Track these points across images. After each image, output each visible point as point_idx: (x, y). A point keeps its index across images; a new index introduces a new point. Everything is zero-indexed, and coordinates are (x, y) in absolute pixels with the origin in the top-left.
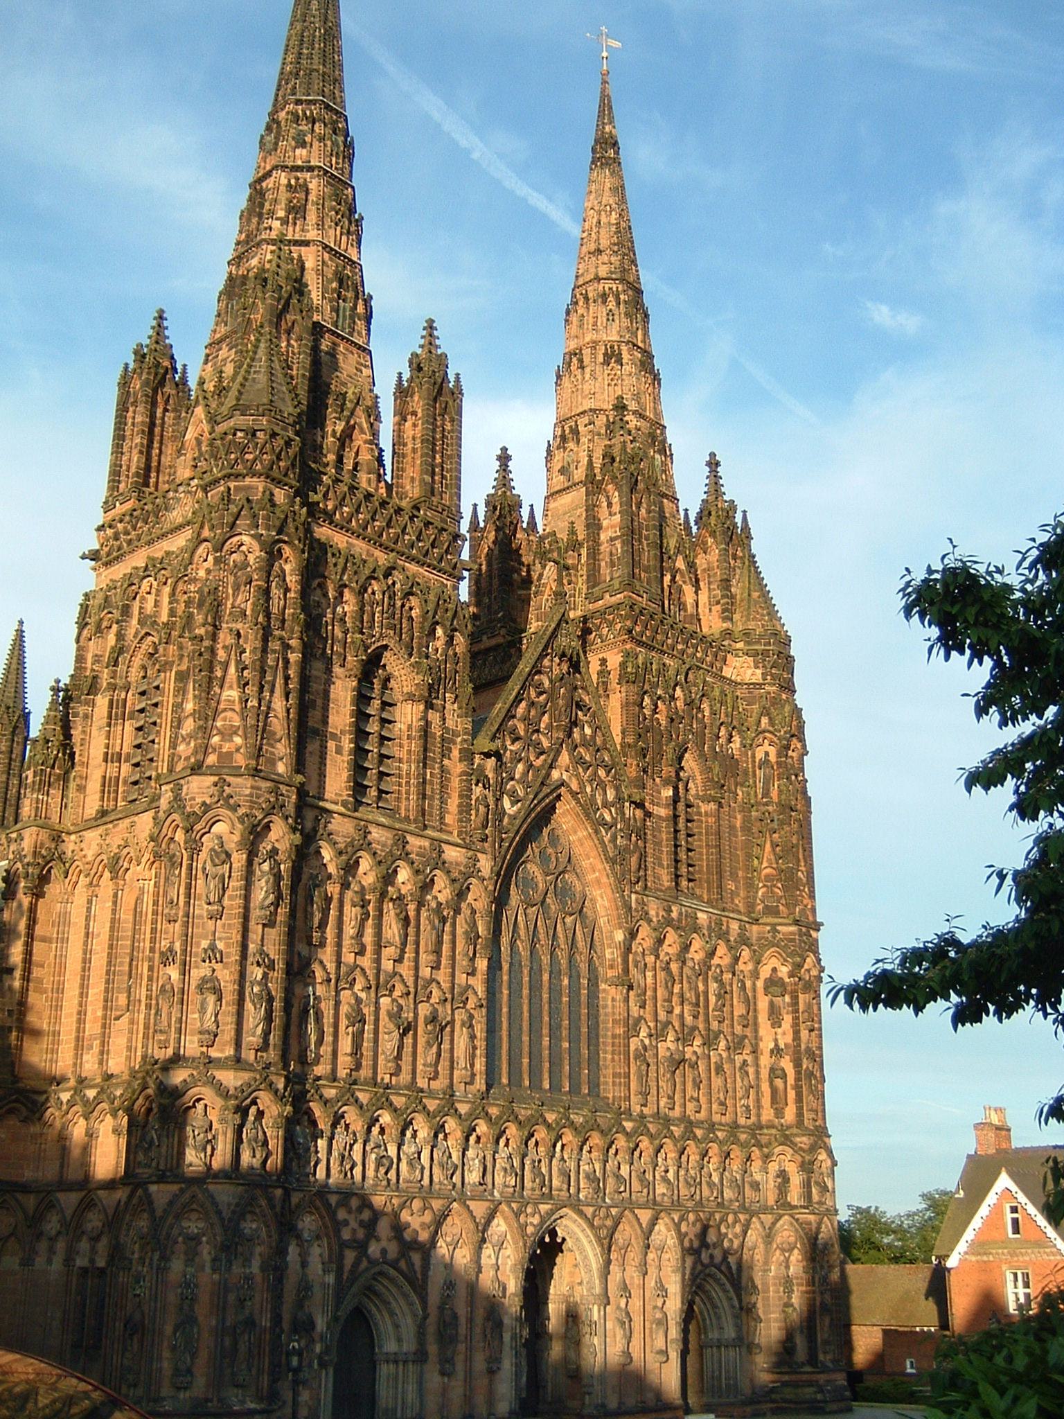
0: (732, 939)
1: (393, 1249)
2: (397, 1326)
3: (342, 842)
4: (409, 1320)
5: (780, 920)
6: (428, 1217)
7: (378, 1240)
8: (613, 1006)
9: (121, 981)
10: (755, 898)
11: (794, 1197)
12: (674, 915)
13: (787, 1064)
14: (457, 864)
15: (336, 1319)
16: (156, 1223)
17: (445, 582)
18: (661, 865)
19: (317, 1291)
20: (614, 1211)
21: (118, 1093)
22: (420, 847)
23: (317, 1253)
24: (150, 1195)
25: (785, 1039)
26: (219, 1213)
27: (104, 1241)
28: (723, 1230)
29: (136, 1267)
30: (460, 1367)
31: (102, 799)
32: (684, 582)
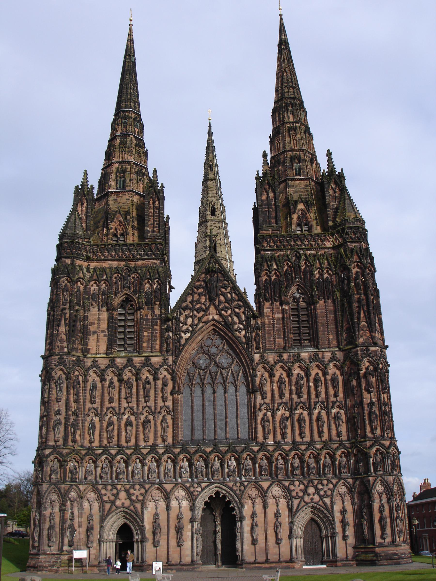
0: (326, 360)
1: (127, 503)
3: (103, 367)
6: (143, 491)
12: (285, 356)
13: (375, 409)
14: (158, 363)
17: (156, 262)
18: (279, 338)
22: (140, 361)
28: (320, 486)
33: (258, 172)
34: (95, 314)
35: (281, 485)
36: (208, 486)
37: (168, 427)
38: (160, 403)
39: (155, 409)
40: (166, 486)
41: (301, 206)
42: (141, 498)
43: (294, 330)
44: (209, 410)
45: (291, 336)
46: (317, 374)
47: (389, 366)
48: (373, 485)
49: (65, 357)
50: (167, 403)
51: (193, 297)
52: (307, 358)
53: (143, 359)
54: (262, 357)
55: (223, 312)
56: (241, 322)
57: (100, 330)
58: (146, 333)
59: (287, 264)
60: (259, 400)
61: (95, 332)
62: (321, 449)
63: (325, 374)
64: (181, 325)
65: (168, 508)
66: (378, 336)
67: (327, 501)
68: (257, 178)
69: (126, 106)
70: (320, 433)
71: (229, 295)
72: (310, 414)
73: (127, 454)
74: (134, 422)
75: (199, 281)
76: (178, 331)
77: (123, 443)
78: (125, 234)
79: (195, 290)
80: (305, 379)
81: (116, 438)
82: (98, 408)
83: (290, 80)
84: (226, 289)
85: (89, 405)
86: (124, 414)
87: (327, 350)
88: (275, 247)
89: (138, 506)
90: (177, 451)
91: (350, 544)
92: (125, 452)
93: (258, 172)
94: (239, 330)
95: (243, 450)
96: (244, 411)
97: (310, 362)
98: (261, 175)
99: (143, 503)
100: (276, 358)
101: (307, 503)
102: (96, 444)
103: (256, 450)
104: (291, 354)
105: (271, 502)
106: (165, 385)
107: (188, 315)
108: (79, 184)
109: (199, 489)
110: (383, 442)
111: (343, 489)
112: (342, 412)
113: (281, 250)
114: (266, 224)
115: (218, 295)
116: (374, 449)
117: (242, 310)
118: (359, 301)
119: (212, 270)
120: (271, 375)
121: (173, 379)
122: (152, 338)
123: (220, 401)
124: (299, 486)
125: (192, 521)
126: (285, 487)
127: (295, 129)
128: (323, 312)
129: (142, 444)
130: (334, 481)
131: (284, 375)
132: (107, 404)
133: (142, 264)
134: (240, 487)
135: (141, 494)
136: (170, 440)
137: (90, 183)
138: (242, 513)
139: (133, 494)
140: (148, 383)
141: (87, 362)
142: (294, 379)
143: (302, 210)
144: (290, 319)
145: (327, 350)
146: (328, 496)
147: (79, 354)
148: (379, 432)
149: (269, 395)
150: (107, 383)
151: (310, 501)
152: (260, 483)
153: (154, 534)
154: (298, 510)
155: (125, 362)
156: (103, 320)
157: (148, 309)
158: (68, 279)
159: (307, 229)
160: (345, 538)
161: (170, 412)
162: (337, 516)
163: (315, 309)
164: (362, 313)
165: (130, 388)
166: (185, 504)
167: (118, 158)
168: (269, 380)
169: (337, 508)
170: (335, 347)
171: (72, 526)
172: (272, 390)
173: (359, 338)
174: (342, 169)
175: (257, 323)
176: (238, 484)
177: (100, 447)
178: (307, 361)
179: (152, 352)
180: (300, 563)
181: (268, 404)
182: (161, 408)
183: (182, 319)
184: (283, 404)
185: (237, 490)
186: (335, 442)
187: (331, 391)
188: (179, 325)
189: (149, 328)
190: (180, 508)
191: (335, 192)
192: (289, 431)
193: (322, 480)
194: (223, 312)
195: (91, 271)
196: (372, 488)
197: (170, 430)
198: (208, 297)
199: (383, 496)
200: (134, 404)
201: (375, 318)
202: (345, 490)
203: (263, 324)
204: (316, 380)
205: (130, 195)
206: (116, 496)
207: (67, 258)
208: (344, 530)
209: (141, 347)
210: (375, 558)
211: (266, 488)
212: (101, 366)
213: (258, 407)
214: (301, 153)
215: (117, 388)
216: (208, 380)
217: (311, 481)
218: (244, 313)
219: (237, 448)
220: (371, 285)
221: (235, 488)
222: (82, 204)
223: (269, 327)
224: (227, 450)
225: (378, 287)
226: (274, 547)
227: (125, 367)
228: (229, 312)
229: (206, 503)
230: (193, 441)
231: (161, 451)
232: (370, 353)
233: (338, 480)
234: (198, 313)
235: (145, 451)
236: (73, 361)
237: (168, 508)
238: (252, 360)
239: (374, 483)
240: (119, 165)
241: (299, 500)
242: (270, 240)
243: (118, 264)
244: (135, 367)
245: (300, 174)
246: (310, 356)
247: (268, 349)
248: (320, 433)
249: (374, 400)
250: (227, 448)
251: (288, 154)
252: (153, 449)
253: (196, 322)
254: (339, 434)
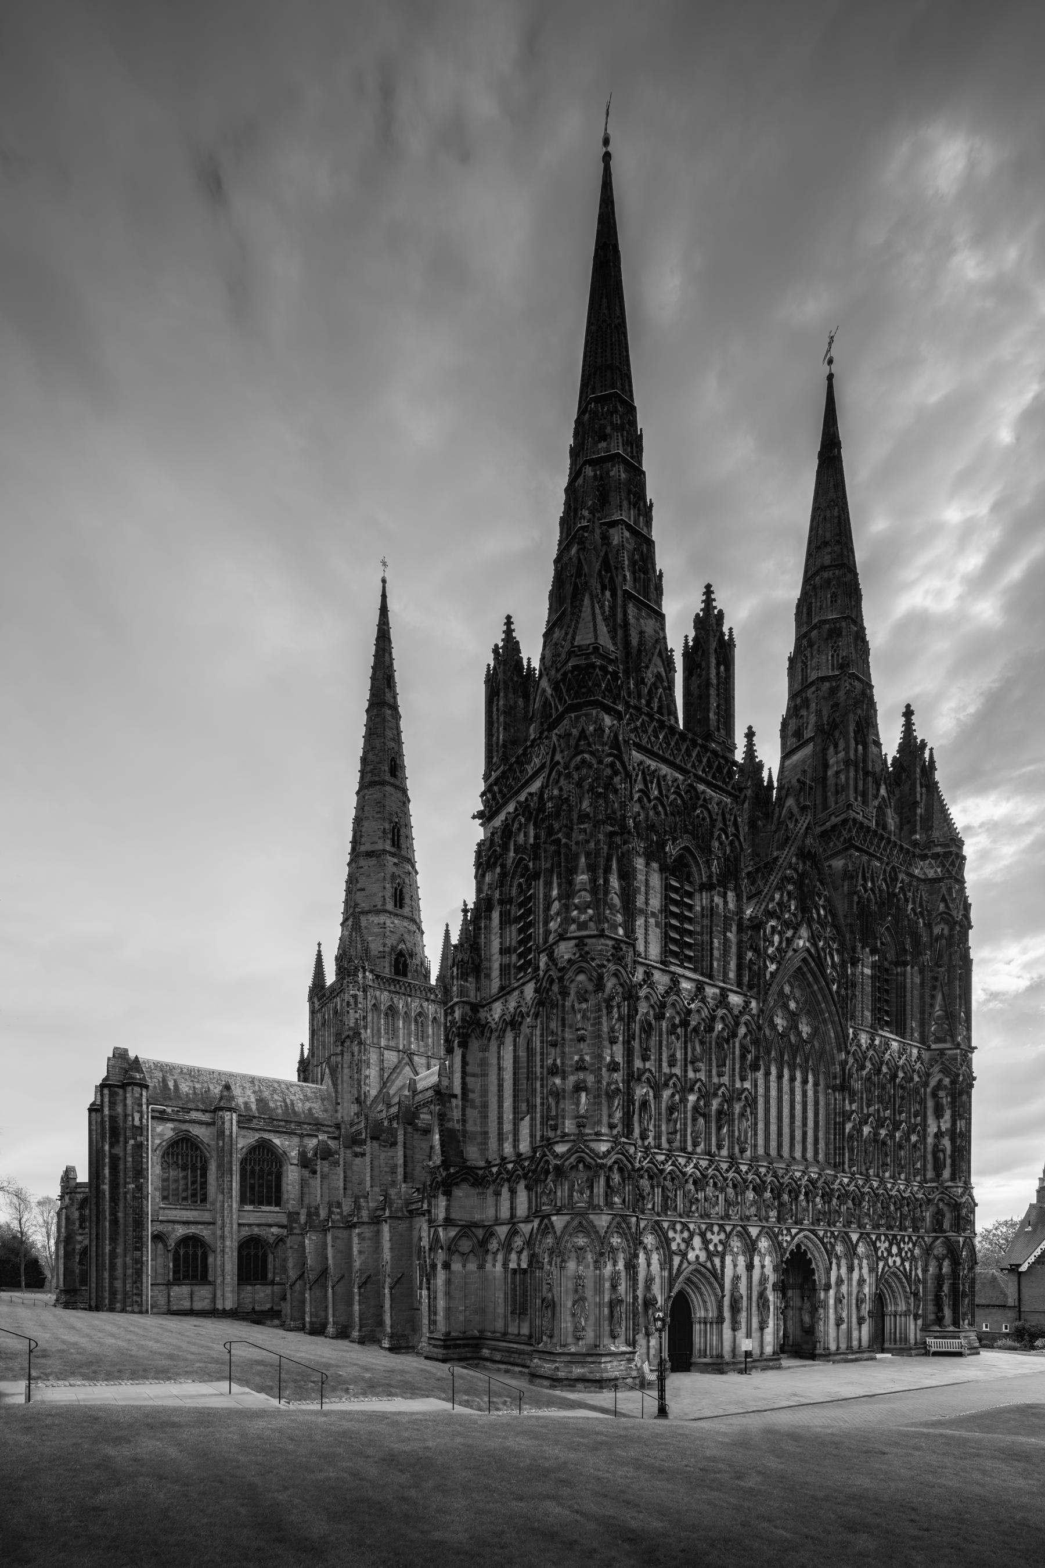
2: (705, 1302)
4: (713, 1298)
6: (722, 1236)
7: (693, 1249)
8: (835, 1104)
9: (523, 1096)
12: (877, 1042)
15: (670, 1297)
16: (558, 1240)
18: (867, 1009)
19: (658, 1280)
21: (526, 1164)
23: (655, 1258)
24: (552, 1223)
26: (597, 1232)
27: (525, 1254)
29: (547, 1267)
30: (744, 1325)
31: (501, 980)
54: (855, 1035)
65: (750, 1267)
89: (717, 1261)
190: (763, 1267)
206: (688, 1242)
237: (750, 1267)
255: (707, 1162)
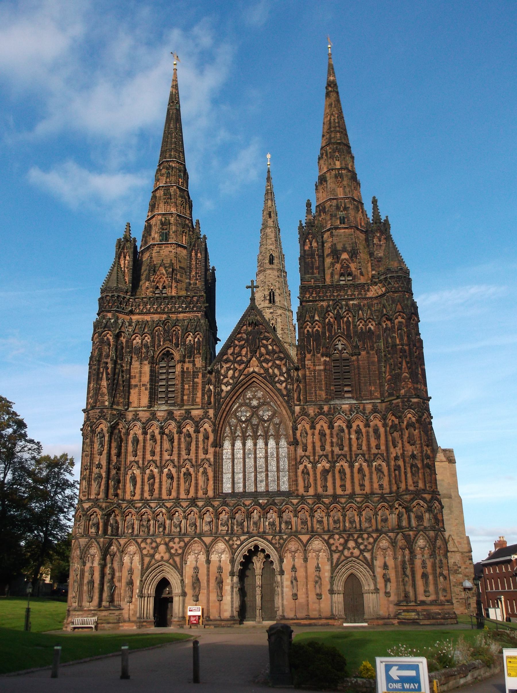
0: (367, 412)
1: (167, 556)
3: (144, 420)
5: (393, 398)
6: (182, 544)
10: (384, 391)
11: (404, 523)
12: (326, 408)
14: (198, 416)
18: (321, 389)
20: (285, 537)
25: (400, 452)
28: (360, 541)
32: (350, 263)
33: (300, 221)
34: (136, 368)
35: (321, 539)
36: (247, 539)
37: (208, 480)
38: (201, 456)
39: (196, 462)
40: (204, 539)
41: (345, 256)
42: (180, 551)
43: (335, 382)
44: (250, 462)
45: (332, 388)
46: (358, 426)
47: (432, 418)
48: (414, 540)
49: (105, 410)
50: (208, 456)
51: (234, 349)
52: (348, 410)
53: (183, 412)
54: (303, 410)
55: (264, 365)
56: (282, 374)
57: (141, 383)
58: (186, 386)
59: (329, 315)
60: (300, 451)
61: (136, 386)
62: (361, 503)
63: (367, 425)
64: (222, 377)
65: (208, 561)
66: (421, 387)
67: (367, 555)
68: (301, 227)
69: (170, 155)
70: (362, 486)
71: (270, 347)
72: (351, 466)
73: (167, 507)
74: (175, 475)
75: (239, 333)
76: (219, 383)
77: (164, 496)
78: (167, 287)
79: (236, 342)
80: (346, 431)
81: (156, 492)
82: (139, 461)
83: (337, 125)
84: (267, 341)
85: (131, 458)
86: (165, 467)
87: (368, 402)
88: (318, 298)
89: (177, 559)
90: (216, 503)
91: (391, 602)
92: (165, 506)
93: (300, 221)
94: (281, 382)
95: (282, 503)
96: (284, 464)
97: (351, 414)
98: (304, 225)
99: (183, 556)
100: (317, 410)
101: (347, 558)
102: (137, 497)
103: (295, 503)
104: (332, 406)
105: (311, 555)
106: (206, 437)
107: (228, 367)
108: (122, 237)
109: (239, 543)
110: (426, 496)
111: (384, 543)
112: (384, 464)
113: (323, 300)
114: (309, 274)
115: (259, 347)
116: (415, 503)
117: (283, 362)
118: (403, 351)
119: (252, 322)
120: (313, 427)
121: (215, 431)
122: (193, 391)
123: (261, 454)
124: (338, 540)
125: (232, 574)
126: (325, 540)
127: (341, 176)
128: (364, 363)
129: (183, 496)
130: (375, 535)
131: (325, 426)
132: (149, 457)
133: (184, 317)
134: (279, 540)
135: (180, 547)
136: (211, 493)
137: (133, 236)
138: (281, 567)
139: (173, 548)
140: (189, 436)
141: (128, 415)
142: (335, 431)
143: (345, 259)
144: (332, 371)
145: (368, 402)
146: (368, 551)
147: (120, 408)
148: (421, 485)
149: (310, 448)
150: (148, 437)
151: (349, 555)
152: (299, 536)
153: (194, 588)
154: (337, 565)
155: (166, 415)
156: (145, 373)
157: (189, 362)
158: (110, 332)
159: (351, 278)
160: (387, 594)
161: (211, 465)
162: (379, 571)
163: (358, 360)
164: (404, 363)
165: (172, 441)
166: (225, 557)
167: (162, 209)
168: (310, 432)
169: (378, 563)
170: (377, 399)
171: (112, 580)
172: (314, 443)
173: (400, 390)
174: (387, 217)
175: (298, 375)
176: (277, 538)
177: (140, 500)
178: (348, 413)
179: (193, 405)
180: (341, 620)
181: (308, 457)
182: (203, 460)
183: (222, 371)
184: (323, 457)
185: (276, 543)
186: (376, 496)
187: (373, 443)
188: (219, 378)
189: (190, 381)
191: (380, 241)
192: (330, 484)
193: (362, 534)
194: (264, 365)
195: (133, 324)
196: (413, 543)
197: (211, 482)
198: (249, 349)
199: (425, 552)
200: (175, 457)
201: (417, 368)
202: (387, 544)
203: (305, 376)
204: (358, 432)
205: (173, 247)
207: (109, 311)
208: (386, 585)
209: (182, 400)
210: (416, 617)
211: (305, 542)
212: (142, 419)
213: (299, 460)
214: (346, 201)
215: (159, 442)
216: (249, 433)
217: (351, 535)
218: (285, 365)
219: (276, 501)
220: (413, 335)
221: (274, 541)
222: (125, 257)
223: (310, 379)
224: (266, 503)
225: (422, 337)
226: (314, 603)
227: (166, 420)
228: (270, 364)
229: (245, 557)
230: (233, 494)
231: (200, 504)
232: (412, 405)
233: (378, 534)
234: (240, 365)
235: (184, 504)
236: (114, 415)
237: (208, 561)
238: (293, 412)
239: (415, 538)
240: (162, 217)
241: (339, 554)
242: (313, 292)
243: (160, 317)
244: (176, 420)
245: (344, 223)
246: (351, 408)
247: (309, 402)
248: (362, 486)
249: (415, 452)
250: (266, 501)
251: (334, 202)
252: (193, 502)
253: (236, 375)
254: (381, 486)
255: (155, 504)
